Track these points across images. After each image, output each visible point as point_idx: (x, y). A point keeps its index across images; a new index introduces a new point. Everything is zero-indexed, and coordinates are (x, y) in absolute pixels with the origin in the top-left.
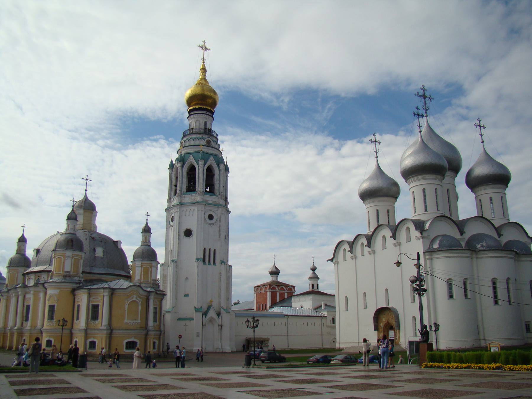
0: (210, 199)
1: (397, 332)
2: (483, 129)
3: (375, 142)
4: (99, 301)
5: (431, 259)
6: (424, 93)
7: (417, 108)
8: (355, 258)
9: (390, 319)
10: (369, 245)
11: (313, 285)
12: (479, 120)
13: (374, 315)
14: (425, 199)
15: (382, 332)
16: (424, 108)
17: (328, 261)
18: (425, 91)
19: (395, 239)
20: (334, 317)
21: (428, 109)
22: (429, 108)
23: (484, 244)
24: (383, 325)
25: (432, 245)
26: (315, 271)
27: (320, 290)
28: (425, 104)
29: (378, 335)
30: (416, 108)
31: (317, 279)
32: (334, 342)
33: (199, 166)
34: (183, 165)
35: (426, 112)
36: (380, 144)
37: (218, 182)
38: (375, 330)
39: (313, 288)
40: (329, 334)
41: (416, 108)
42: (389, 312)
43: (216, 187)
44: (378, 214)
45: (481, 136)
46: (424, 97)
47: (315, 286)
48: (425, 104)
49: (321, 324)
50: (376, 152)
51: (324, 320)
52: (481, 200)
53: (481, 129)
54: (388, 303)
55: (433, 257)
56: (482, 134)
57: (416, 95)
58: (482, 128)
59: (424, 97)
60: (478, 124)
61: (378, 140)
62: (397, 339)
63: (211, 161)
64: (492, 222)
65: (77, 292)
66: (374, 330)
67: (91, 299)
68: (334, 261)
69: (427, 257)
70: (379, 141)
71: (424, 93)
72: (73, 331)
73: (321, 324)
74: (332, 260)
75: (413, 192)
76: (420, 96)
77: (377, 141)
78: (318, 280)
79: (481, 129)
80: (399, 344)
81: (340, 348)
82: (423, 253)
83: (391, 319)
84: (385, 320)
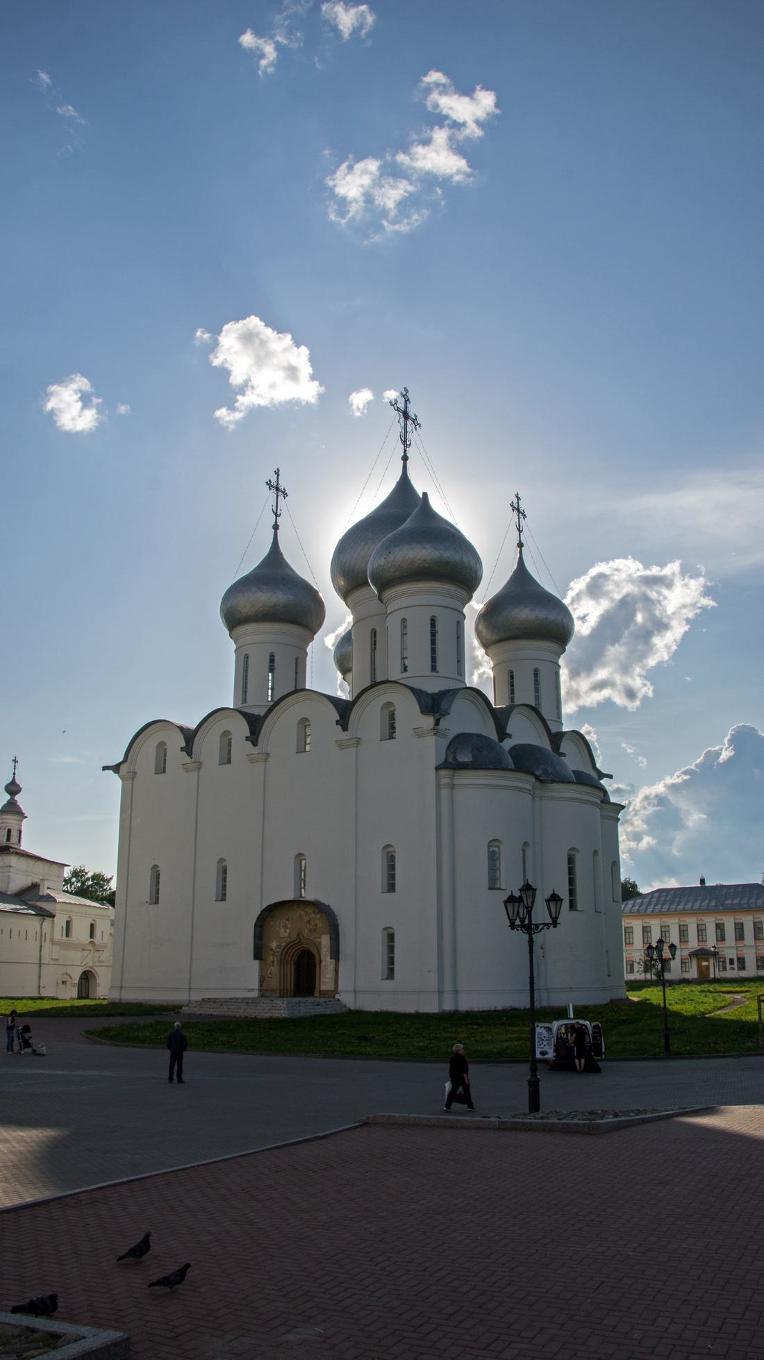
1: (326, 965)
3: (277, 489)
5: (452, 786)
6: (406, 407)
8: (199, 766)
9: (307, 931)
11: (9, 831)
13: (258, 918)
14: (433, 642)
15: (276, 962)
17: (105, 768)
19: (345, 728)
20: (69, 919)
23: (550, 769)
24: (280, 945)
25: (455, 753)
26: (16, 798)
27: (25, 846)
28: (406, 432)
29: (261, 969)
31: (20, 818)
32: (63, 982)
35: (405, 451)
36: (285, 498)
38: (255, 958)
39: (9, 839)
40: (56, 963)
42: (303, 913)
44: (274, 666)
45: (518, 532)
46: (406, 415)
47: (14, 834)
49: (41, 936)
50: (277, 515)
51: (47, 923)
52: (512, 672)
55: (457, 781)
58: (521, 515)
59: (406, 415)
61: (272, 491)
62: (325, 983)
64: (548, 722)
66: (254, 959)
68: (123, 768)
69: (445, 781)
73: (41, 936)
74: (116, 768)
75: (404, 620)
76: (398, 409)
77: (280, 488)
78: (21, 821)
80: (334, 997)
81: (120, 999)
82: (434, 770)
83: (310, 931)
84: (287, 934)
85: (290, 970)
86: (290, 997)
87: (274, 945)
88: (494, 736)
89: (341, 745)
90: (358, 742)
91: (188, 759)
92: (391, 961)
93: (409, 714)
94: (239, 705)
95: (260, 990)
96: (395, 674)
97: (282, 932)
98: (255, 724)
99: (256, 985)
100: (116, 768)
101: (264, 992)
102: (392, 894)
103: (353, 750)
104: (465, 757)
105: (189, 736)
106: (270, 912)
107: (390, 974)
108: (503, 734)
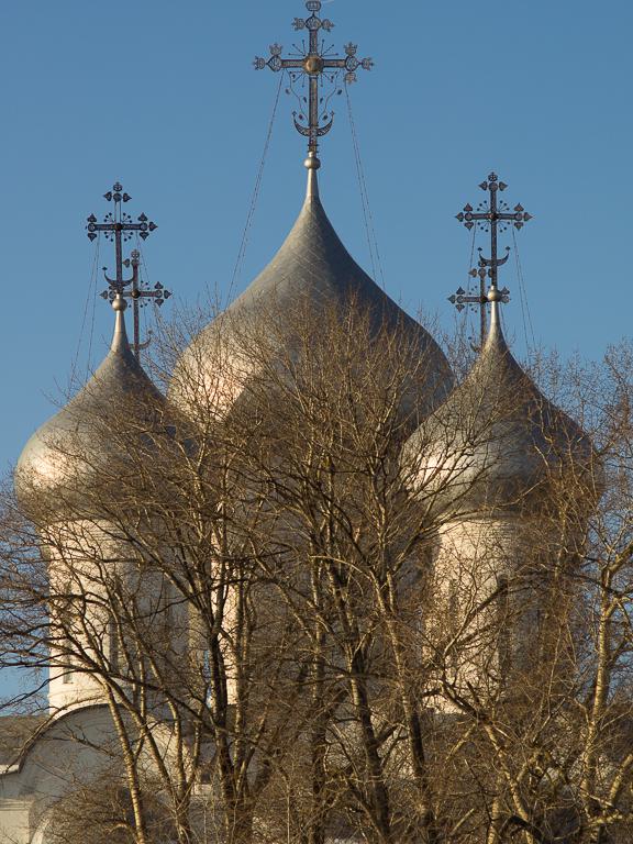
2: (511, 227)
7: (118, 195)
12: (493, 185)
16: (305, 124)
18: (322, 33)
21: (329, 126)
22: (329, 126)
28: (313, 101)
30: (108, 196)
41: (108, 196)
48: (313, 101)
53: (494, 234)
56: (500, 256)
57: (259, 64)
60: (485, 209)
70: (158, 286)
71: (312, 47)
79: (494, 234)
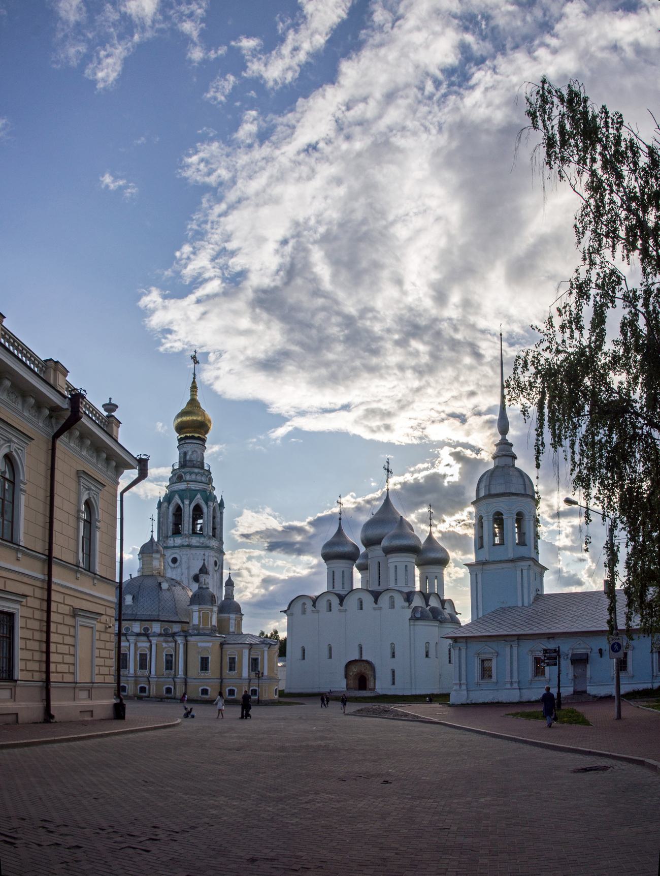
0: (213, 543)
4: (258, 655)
5: (414, 625)
8: (318, 612)
10: (341, 604)
29: (347, 682)
33: (208, 508)
34: (190, 503)
37: (219, 526)
43: (218, 532)
54: (361, 657)
55: (416, 623)
63: (199, 499)
65: (226, 646)
67: (251, 653)
69: (412, 623)
72: (188, 680)
74: (285, 612)
75: (396, 566)
85: (357, 682)
86: (355, 690)
87: (351, 674)
88: (424, 606)
89: (375, 609)
90: (380, 608)
91: (314, 609)
92: (394, 679)
93: (399, 601)
94: (331, 589)
95: (347, 688)
96: (392, 585)
97: (355, 670)
98: (342, 599)
99: (345, 687)
100: (285, 612)
101: (348, 689)
102: (393, 659)
103: (379, 611)
104: (418, 615)
105: (315, 601)
106: (350, 663)
107: (394, 683)
108: (427, 605)
